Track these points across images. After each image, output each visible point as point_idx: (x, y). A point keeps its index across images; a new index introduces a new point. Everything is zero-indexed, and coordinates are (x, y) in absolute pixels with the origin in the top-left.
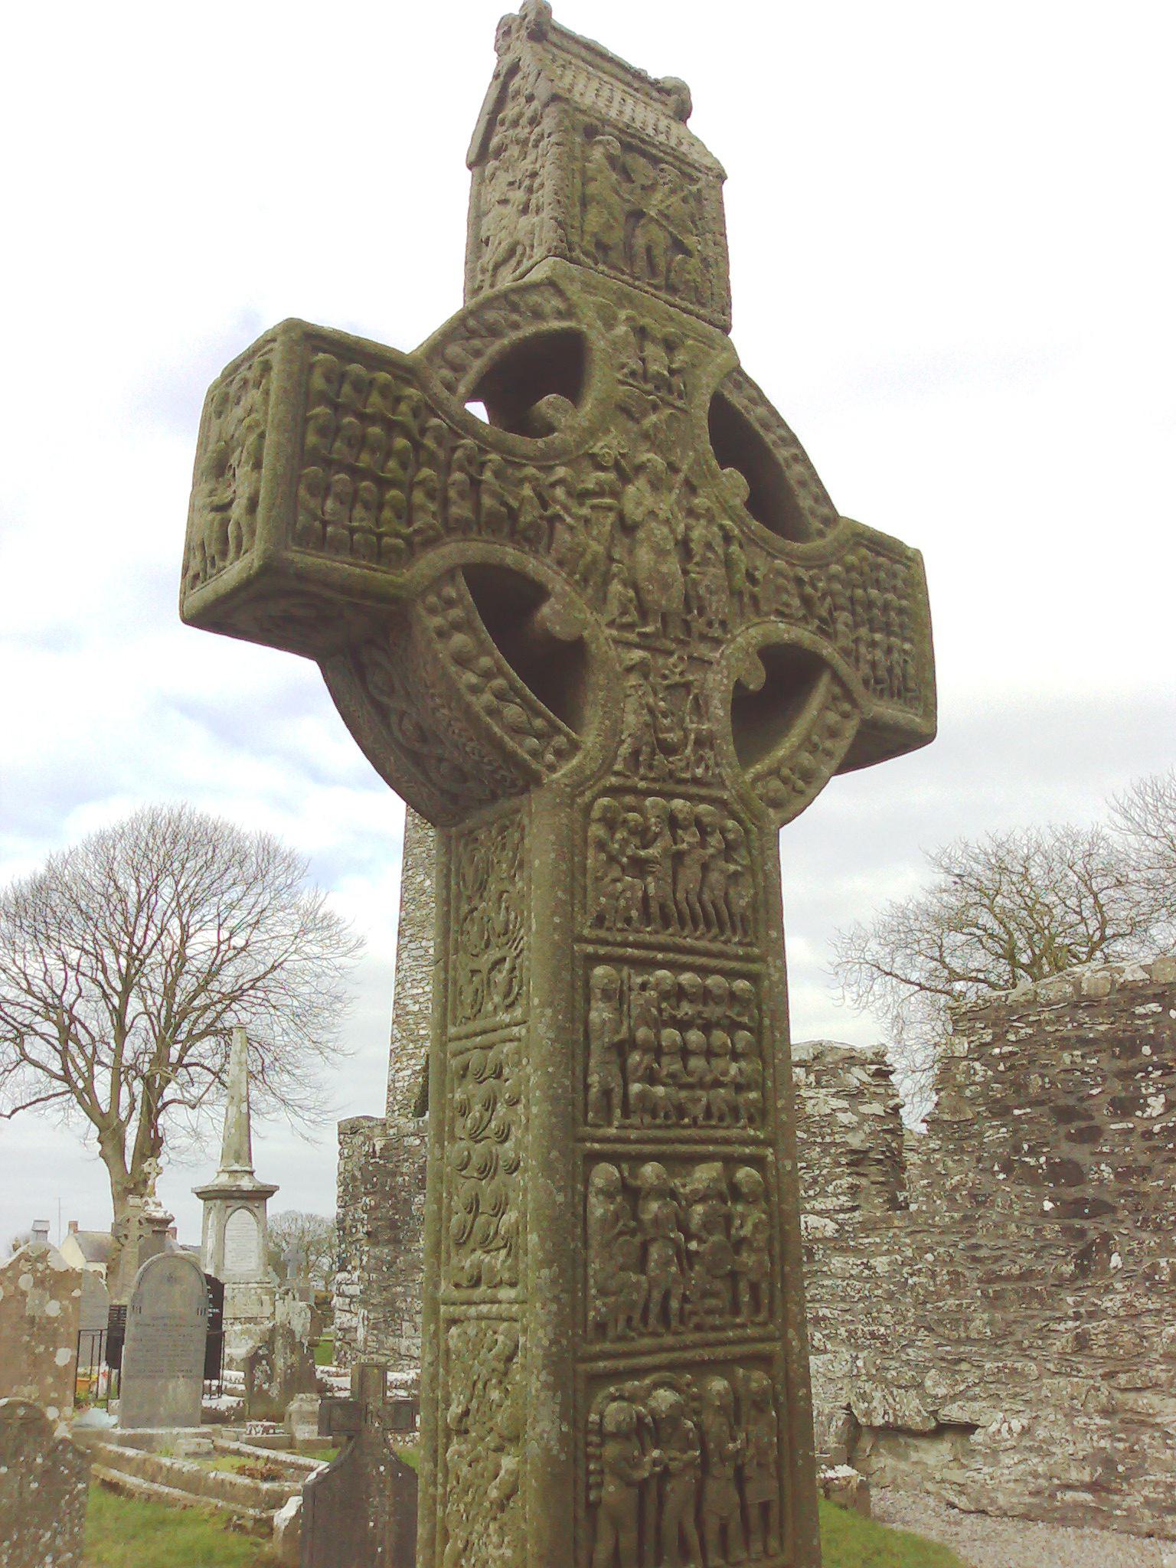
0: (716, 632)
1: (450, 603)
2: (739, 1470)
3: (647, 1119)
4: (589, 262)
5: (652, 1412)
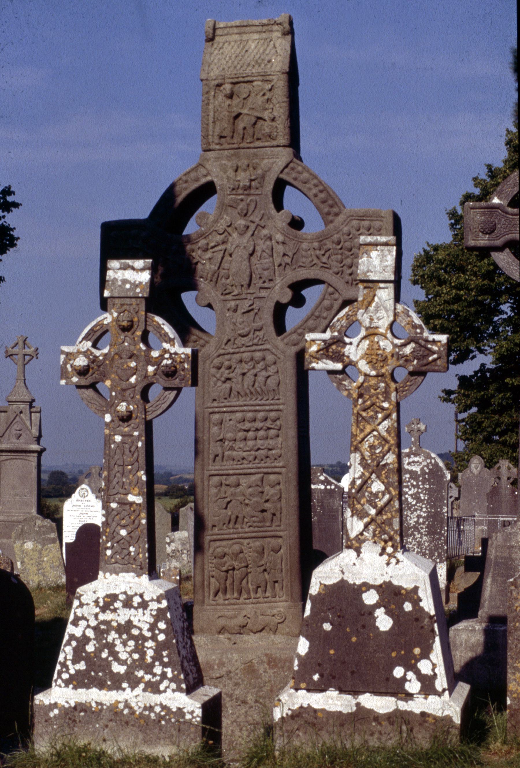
3: (232, 462)
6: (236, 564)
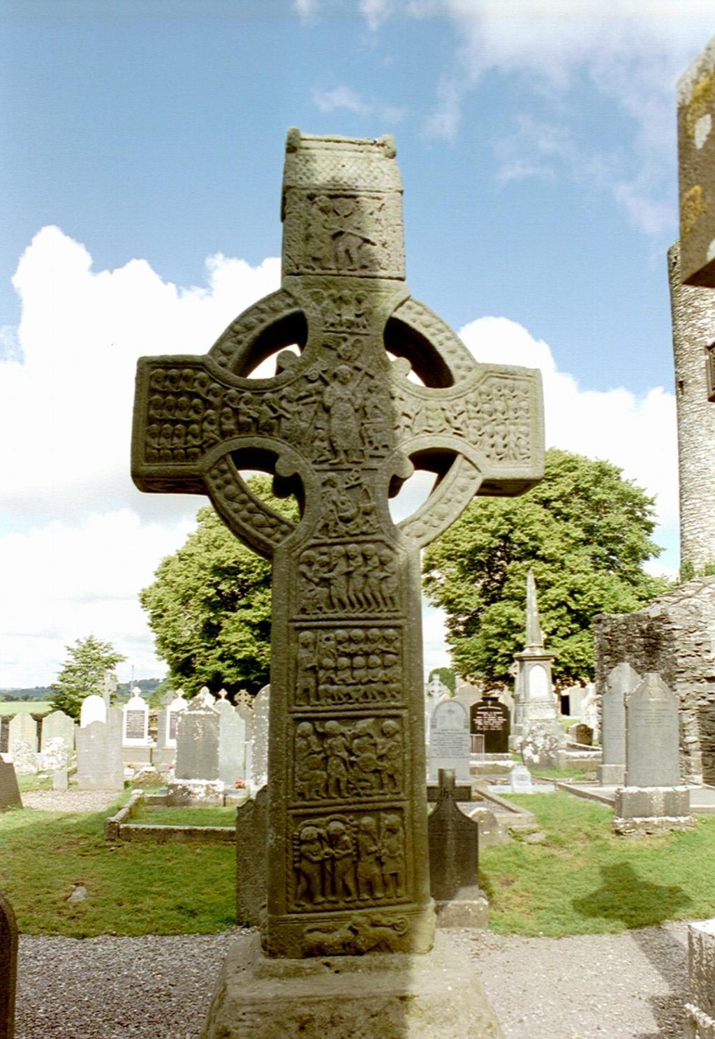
0: (382, 452)
2: (378, 859)
3: (330, 701)
4: (310, 271)
5: (328, 833)
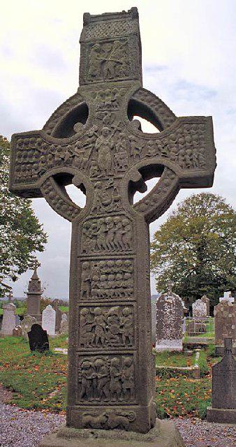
0: (123, 169)
1: (49, 185)
2: (120, 380)
4: (90, 82)
6: (99, 375)
